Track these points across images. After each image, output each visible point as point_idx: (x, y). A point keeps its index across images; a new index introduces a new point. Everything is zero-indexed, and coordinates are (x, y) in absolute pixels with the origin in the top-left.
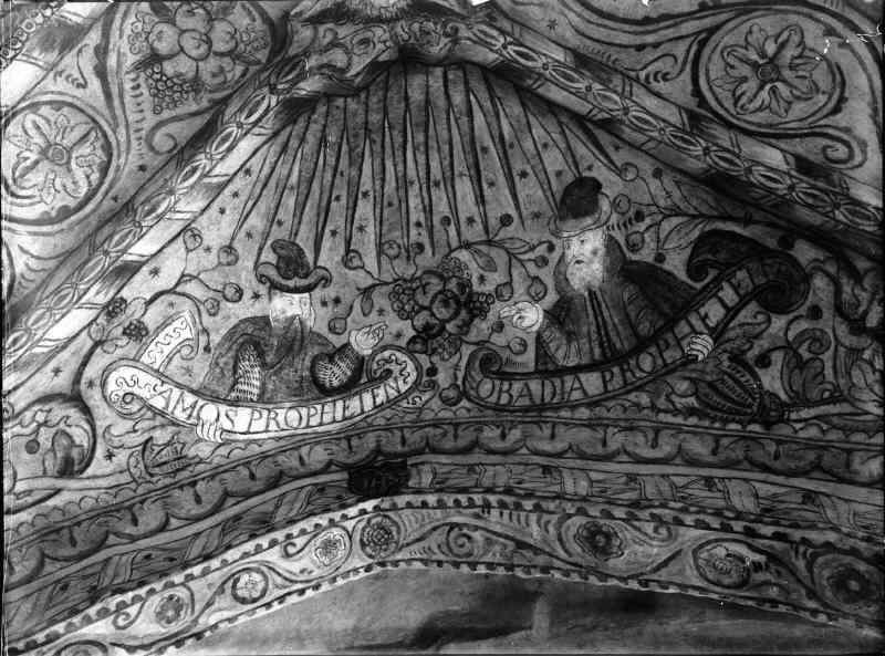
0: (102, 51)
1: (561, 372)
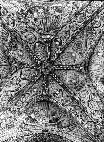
0: (70, 35)
1: (38, 7)
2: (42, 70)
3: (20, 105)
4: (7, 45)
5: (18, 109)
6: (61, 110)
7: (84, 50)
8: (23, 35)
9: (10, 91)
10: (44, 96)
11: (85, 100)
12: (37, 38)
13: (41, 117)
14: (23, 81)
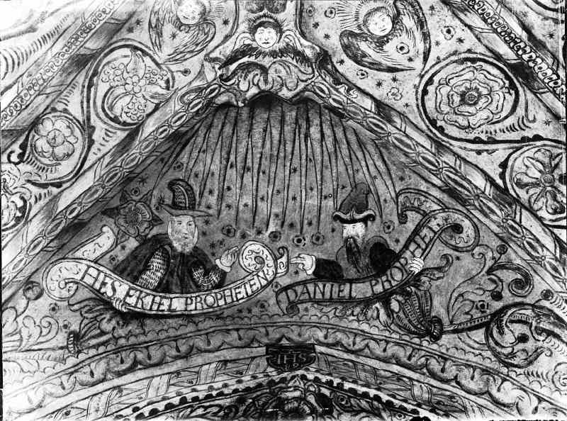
6: (413, 181)
10: (266, 61)
13: (251, 233)
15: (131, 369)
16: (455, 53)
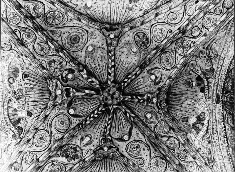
0: (56, 55)
2: (115, 103)
3: (174, 141)
4: (72, 163)
5: (180, 146)
6: (184, 72)
7: (83, 31)
8: (56, 135)
9: (150, 159)
10: (159, 101)
11: (166, 31)
12: (61, 111)
13: (194, 106)
14: (133, 137)
15: (217, 132)
16: (159, 63)
